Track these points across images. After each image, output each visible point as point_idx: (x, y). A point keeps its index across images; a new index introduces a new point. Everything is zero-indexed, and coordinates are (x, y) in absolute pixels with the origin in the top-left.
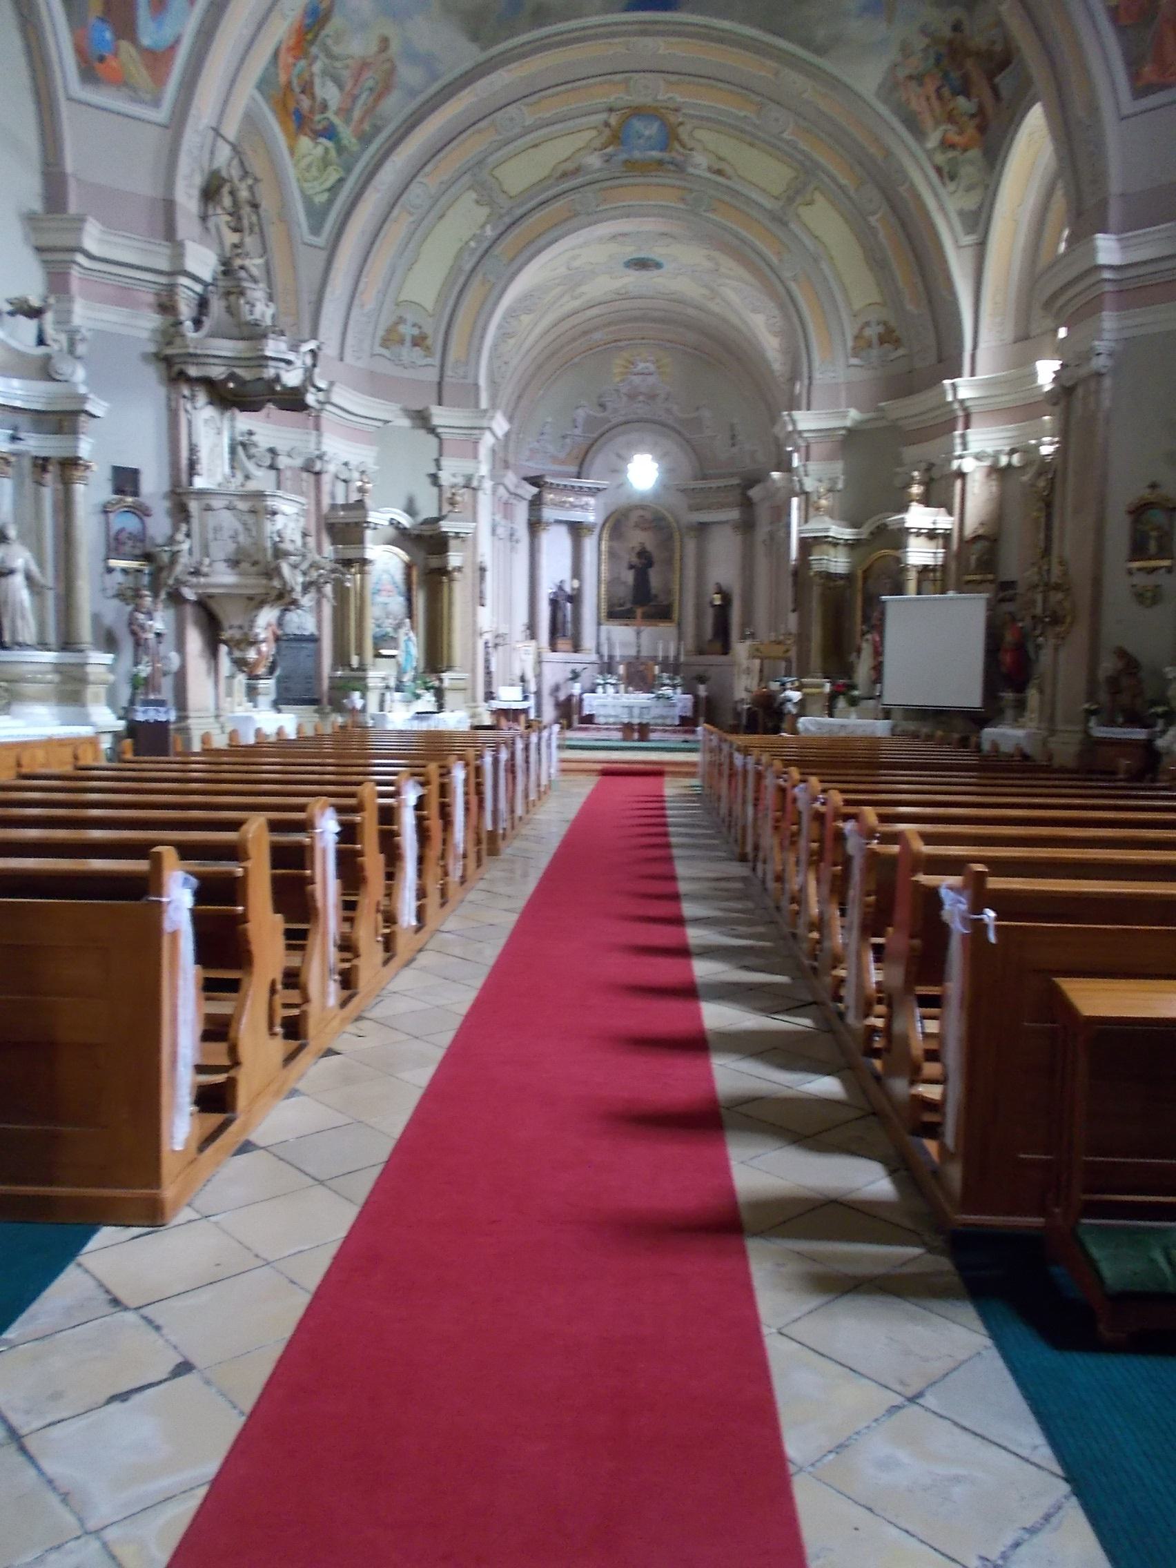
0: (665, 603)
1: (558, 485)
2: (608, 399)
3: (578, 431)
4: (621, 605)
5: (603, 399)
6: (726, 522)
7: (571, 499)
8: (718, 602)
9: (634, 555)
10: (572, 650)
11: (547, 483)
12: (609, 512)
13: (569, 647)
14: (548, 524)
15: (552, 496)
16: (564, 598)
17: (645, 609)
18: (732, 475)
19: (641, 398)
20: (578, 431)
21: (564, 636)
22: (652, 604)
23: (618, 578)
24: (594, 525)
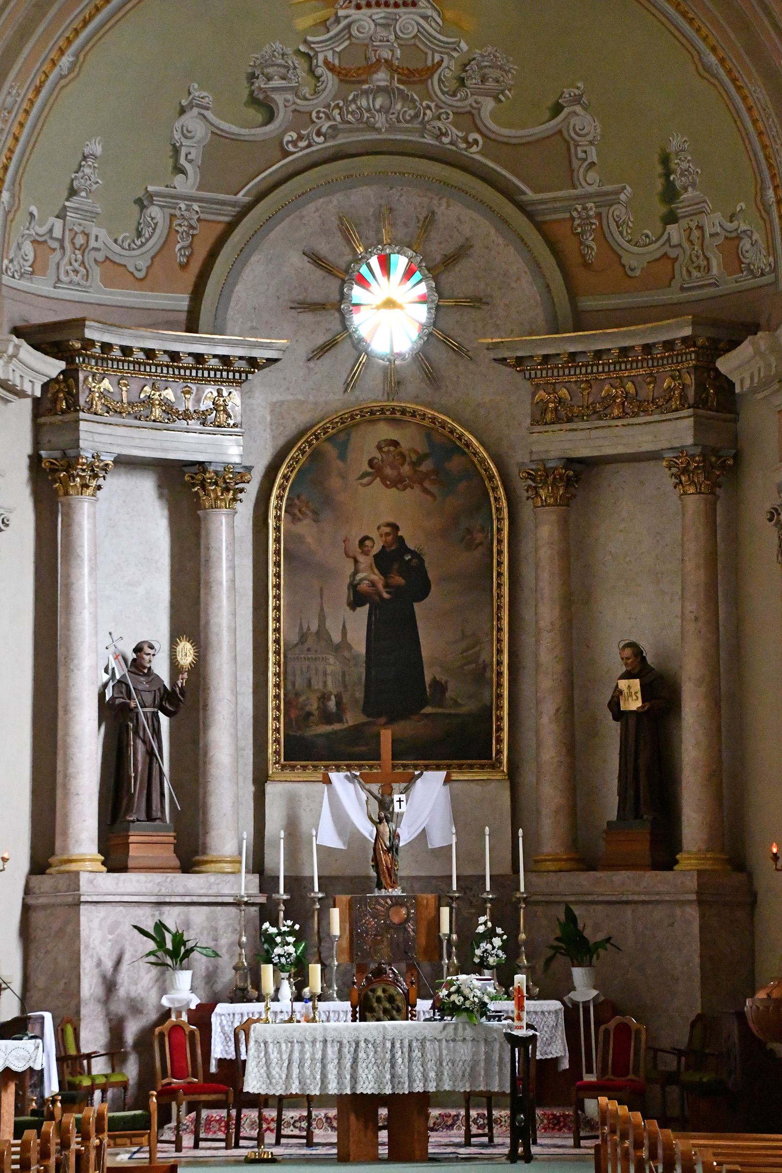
0: (468, 707)
1: (126, 351)
2: (277, 83)
3: (186, 185)
4: (328, 718)
5: (261, 83)
6: (654, 456)
7: (169, 394)
8: (634, 704)
9: (365, 561)
10: (176, 863)
11: (91, 343)
12: (291, 429)
13: (168, 855)
14: (97, 470)
15: (106, 384)
16: (148, 698)
17: (408, 728)
18: (671, 311)
19: (381, 78)
20: (186, 185)
21: (150, 818)
22: (428, 710)
23: (322, 634)
24: (243, 473)
